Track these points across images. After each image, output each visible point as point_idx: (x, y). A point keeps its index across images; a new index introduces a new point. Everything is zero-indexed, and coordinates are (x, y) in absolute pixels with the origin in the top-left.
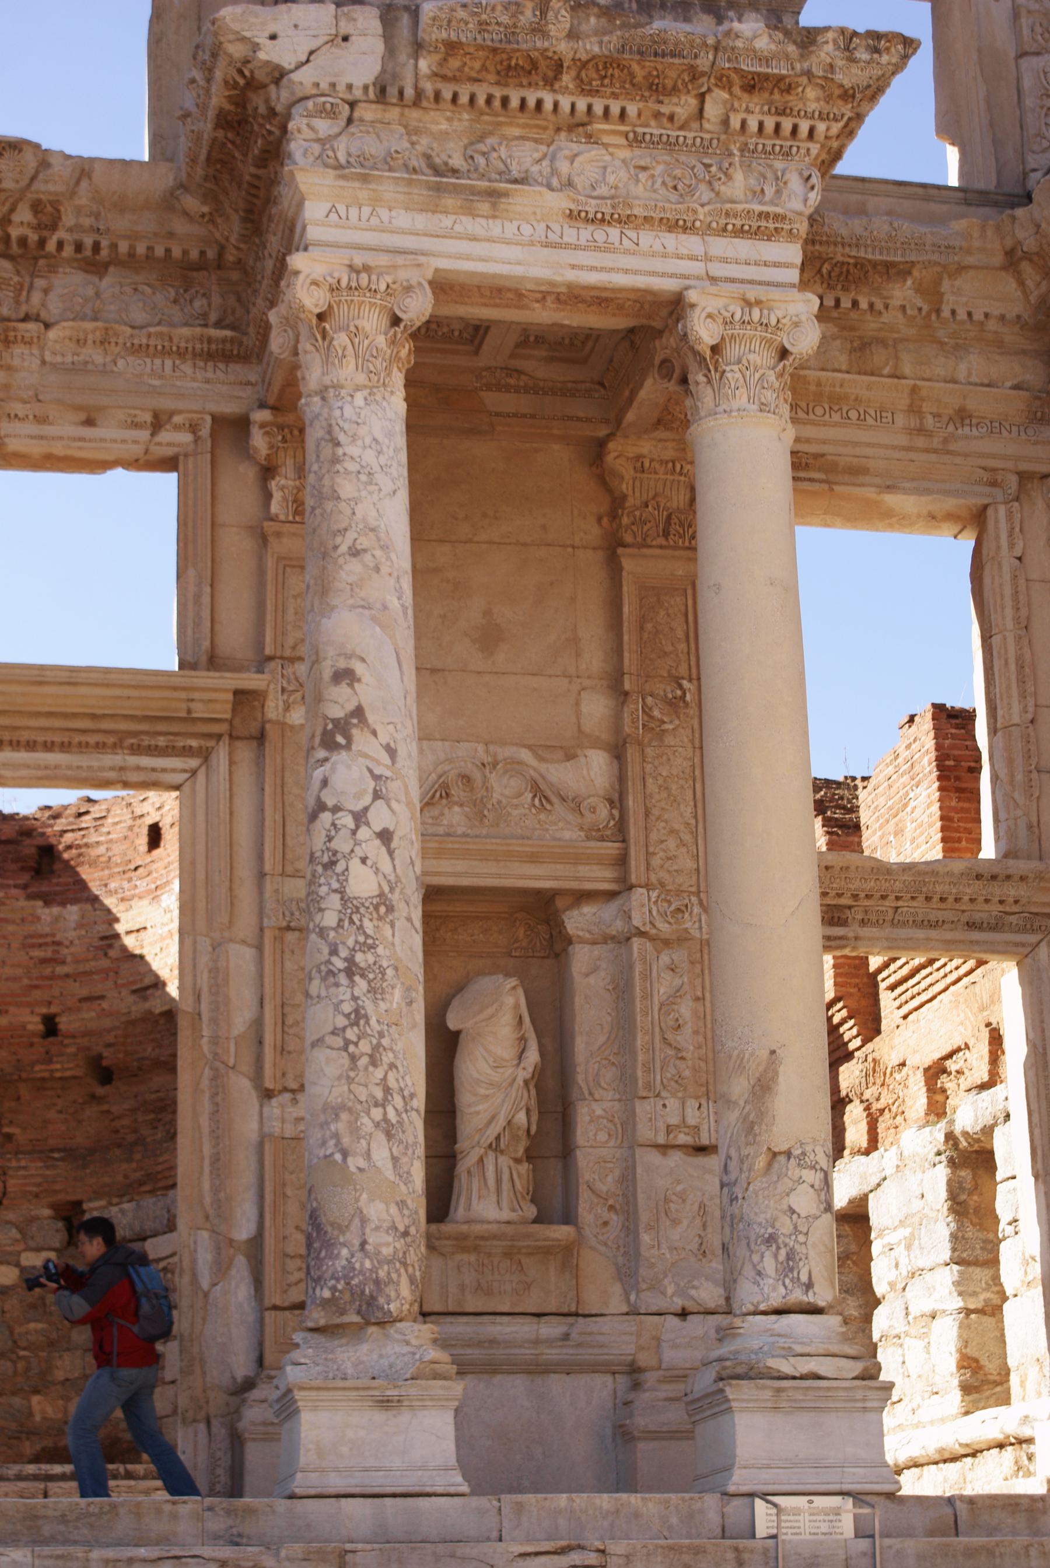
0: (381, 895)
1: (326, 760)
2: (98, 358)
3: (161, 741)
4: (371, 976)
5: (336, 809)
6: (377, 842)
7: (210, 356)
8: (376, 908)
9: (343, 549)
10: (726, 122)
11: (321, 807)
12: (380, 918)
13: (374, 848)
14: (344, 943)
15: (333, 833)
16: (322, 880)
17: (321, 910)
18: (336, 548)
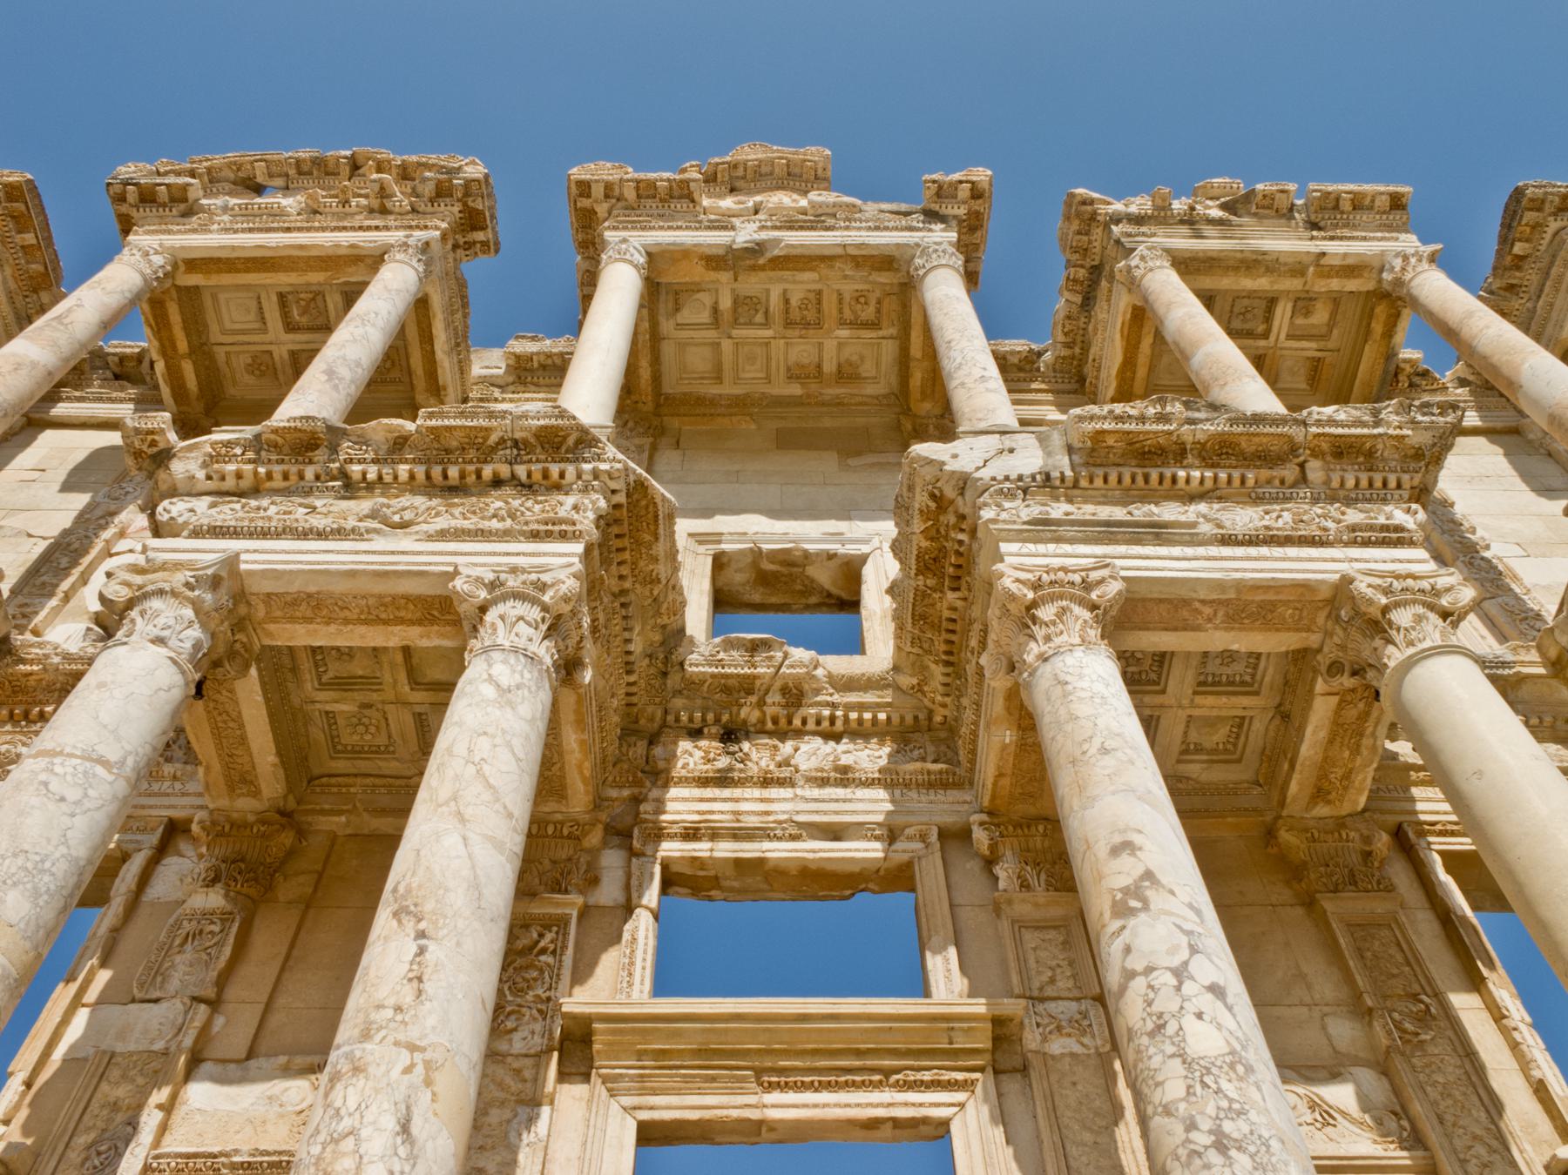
0: (1233, 1053)
1: (1124, 927)
2: (840, 792)
3: (927, 1076)
4: (1252, 1149)
5: (1149, 970)
6: (1210, 996)
7: (930, 785)
8: (1232, 1066)
9: (1093, 751)
10: (1327, 482)
11: (1130, 975)
12: (1241, 1079)
13: (1207, 1002)
14: (1202, 1113)
15: (1152, 995)
16: (1152, 1050)
17: (1158, 1084)
18: (1084, 753)
